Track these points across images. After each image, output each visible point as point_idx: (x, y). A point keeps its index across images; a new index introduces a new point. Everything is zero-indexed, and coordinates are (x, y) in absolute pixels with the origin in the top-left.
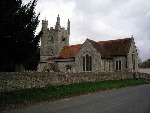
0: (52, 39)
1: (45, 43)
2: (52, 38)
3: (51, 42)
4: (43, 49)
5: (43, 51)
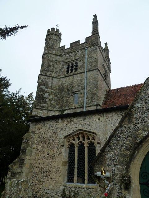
0: (76, 66)
1: (53, 77)
2: (77, 63)
3: (72, 74)
4: (46, 92)
5: (44, 96)
